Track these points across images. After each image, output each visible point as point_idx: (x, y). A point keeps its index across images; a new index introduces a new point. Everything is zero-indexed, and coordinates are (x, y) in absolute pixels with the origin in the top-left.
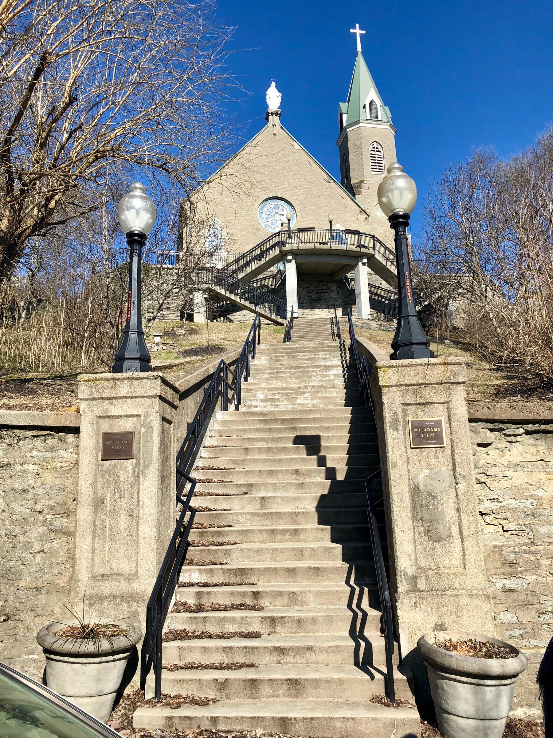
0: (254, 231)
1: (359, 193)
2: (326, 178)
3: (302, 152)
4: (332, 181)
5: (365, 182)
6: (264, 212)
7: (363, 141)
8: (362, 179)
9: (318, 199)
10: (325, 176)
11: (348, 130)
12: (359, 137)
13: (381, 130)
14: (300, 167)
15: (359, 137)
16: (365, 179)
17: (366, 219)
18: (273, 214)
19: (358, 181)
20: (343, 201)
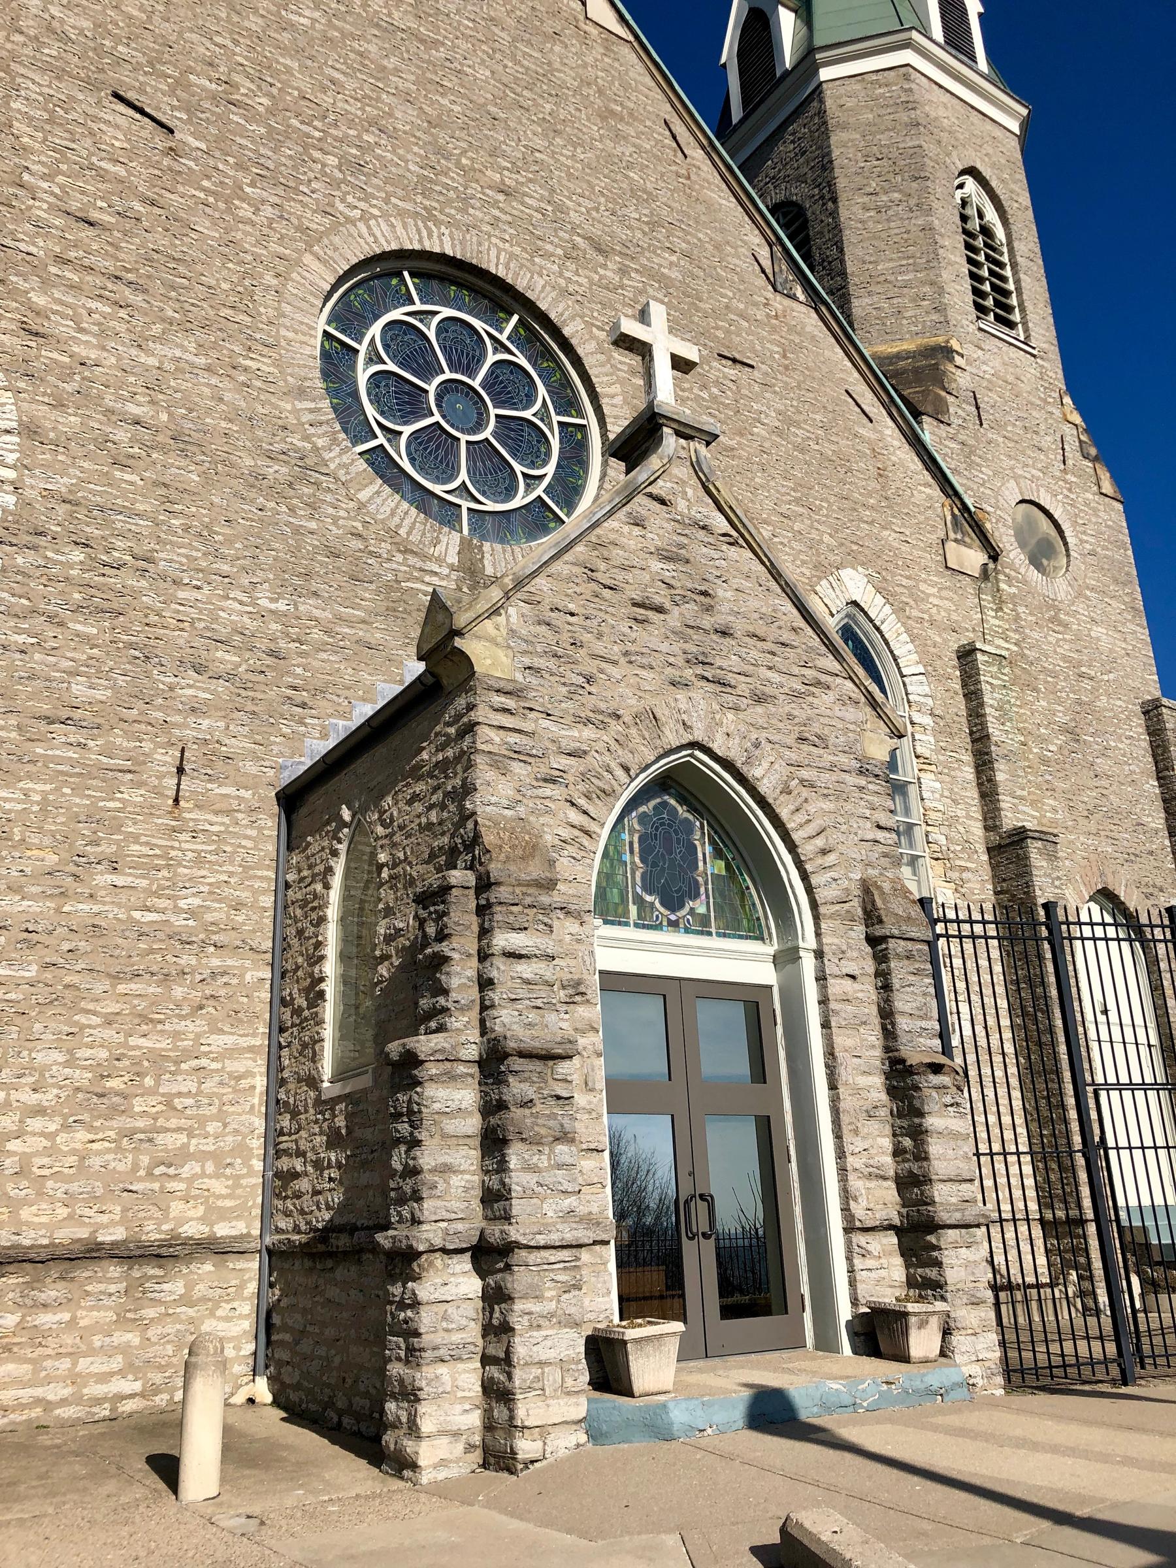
0: (277, 471)
1: (940, 415)
2: (767, 264)
3: (629, 56)
4: (799, 292)
5: (958, 360)
6: (363, 348)
7: (931, 149)
8: (941, 340)
9: (732, 371)
10: (764, 253)
11: (825, 74)
12: (904, 117)
13: (989, 126)
14: (618, 137)
15: (904, 117)
16: (955, 344)
17: (985, 574)
18: (432, 388)
19: (909, 346)
20: (866, 431)
